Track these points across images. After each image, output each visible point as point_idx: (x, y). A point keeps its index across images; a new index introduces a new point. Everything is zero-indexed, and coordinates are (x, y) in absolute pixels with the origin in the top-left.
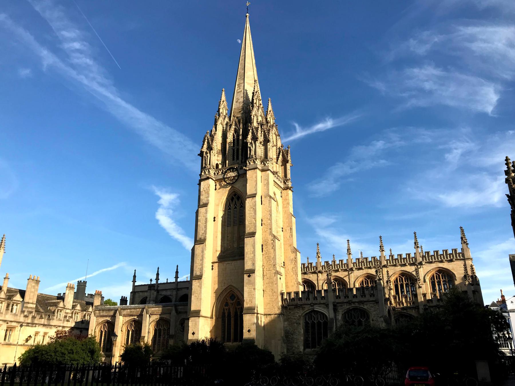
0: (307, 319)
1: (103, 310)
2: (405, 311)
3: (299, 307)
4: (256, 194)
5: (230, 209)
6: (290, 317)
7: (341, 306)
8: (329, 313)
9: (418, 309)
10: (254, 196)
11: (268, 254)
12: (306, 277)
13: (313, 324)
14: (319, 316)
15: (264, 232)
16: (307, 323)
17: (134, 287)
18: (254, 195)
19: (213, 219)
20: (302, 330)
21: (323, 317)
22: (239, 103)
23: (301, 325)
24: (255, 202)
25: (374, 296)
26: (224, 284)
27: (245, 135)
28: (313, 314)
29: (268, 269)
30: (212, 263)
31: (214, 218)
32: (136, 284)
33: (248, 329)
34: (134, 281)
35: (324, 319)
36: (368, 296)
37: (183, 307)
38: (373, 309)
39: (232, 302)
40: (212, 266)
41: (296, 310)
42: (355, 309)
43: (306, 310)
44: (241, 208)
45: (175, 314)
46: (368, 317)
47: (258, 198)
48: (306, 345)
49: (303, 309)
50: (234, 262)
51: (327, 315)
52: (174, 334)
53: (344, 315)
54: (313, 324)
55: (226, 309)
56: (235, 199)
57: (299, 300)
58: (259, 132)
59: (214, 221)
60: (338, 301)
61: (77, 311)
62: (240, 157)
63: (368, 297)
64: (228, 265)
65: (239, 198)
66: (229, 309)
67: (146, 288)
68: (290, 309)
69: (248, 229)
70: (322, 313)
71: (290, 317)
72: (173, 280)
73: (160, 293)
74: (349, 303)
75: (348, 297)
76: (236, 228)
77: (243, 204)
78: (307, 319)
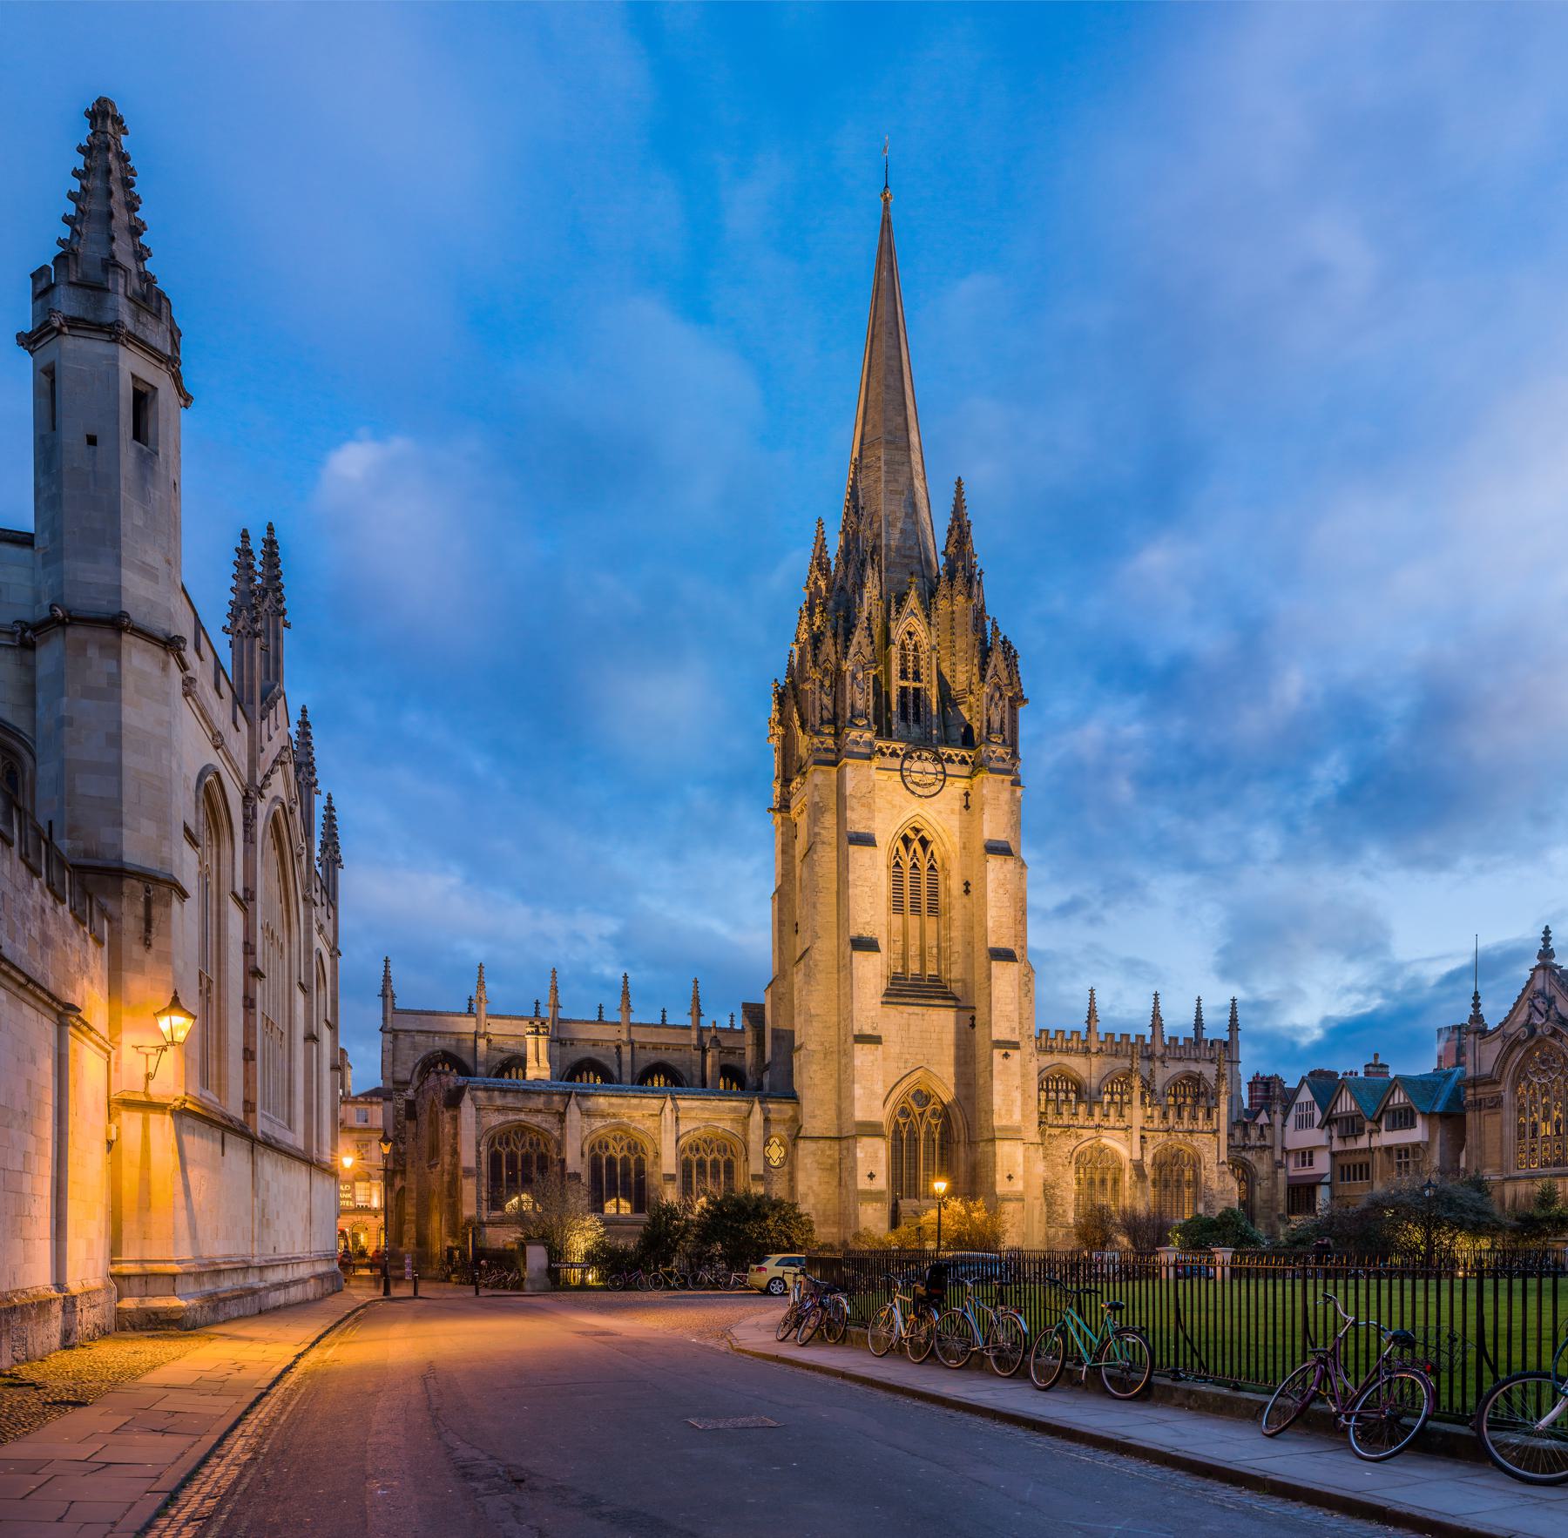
26: (905, 1062)
41: (1063, 1139)
56: (916, 845)
64: (915, 1017)
65: (924, 843)
69: (994, 939)
71: (1049, 1152)
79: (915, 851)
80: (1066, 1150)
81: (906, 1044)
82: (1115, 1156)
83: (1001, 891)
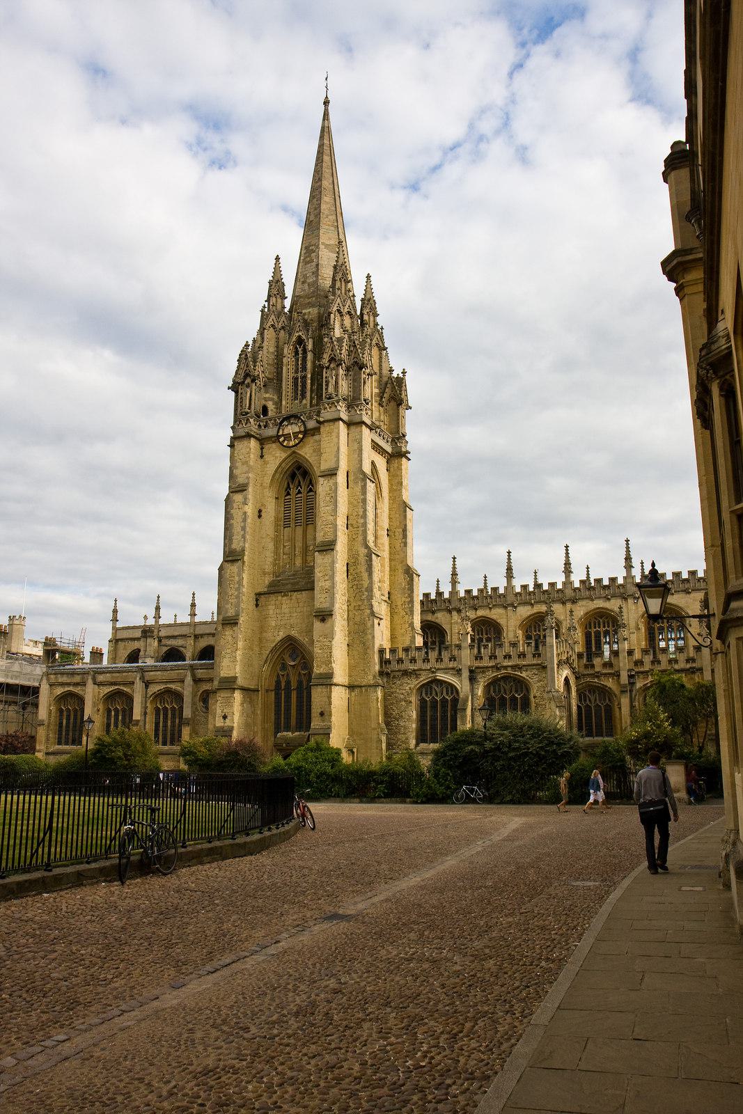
0: (424, 695)
1: (62, 674)
2: (596, 680)
3: (410, 673)
4: (337, 469)
5: (288, 494)
6: (393, 690)
7: (483, 672)
8: (462, 685)
9: (619, 676)
10: (332, 473)
11: (358, 581)
12: (430, 617)
13: (434, 702)
14: (445, 689)
15: (352, 540)
16: (423, 704)
17: (115, 630)
18: (333, 472)
19: (257, 513)
20: (414, 712)
21: (452, 690)
22: (309, 285)
23: (413, 705)
24: (336, 484)
25: (539, 655)
27: (318, 353)
28: (434, 686)
29: (357, 608)
30: (256, 594)
31: (260, 511)
32: (119, 625)
33: (319, 711)
34: (115, 620)
35: (452, 693)
36: (529, 656)
37: (205, 671)
38: (536, 678)
39: (292, 663)
40: (257, 600)
41: (406, 680)
42: (506, 678)
43: (422, 679)
44: (311, 494)
45: (192, 683)
46: (528, 690)
47: (341, 478)
48: (421, 738)
49: (417, 676)
50: (296, 593)
51: (459, 688)
52: (190, 716)
53: (487, 688)
54: (434, 702)
55: (283, 675)
57: (411, 662)
58: (345, 347)
59: (260, 516)
60: (477, 664)
61: (15, 673)
62: (308, 394)
63: (529, 660)
66: (288, 675)
67: (138, 634)
68: (394, 677)
69: (322, 534)
70: (450, 684)
72: (187, 619)
73: (164, 642)
74: (497, 668)
75: (496, 657)
76: (299, 530)
77: (312, 486)
78: (424, 695)
79: (299, 482)
80: (407, 688)
81: (280, 618)
82: (451, 687)
83: (328, 499)
